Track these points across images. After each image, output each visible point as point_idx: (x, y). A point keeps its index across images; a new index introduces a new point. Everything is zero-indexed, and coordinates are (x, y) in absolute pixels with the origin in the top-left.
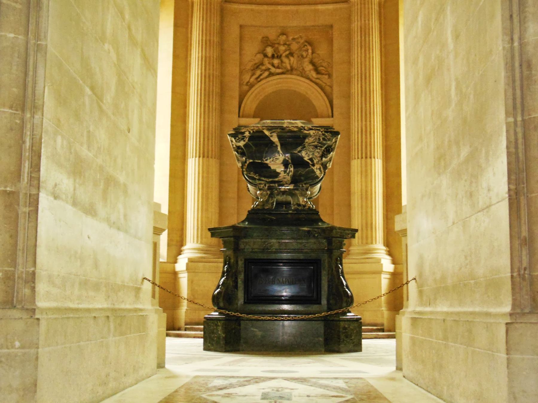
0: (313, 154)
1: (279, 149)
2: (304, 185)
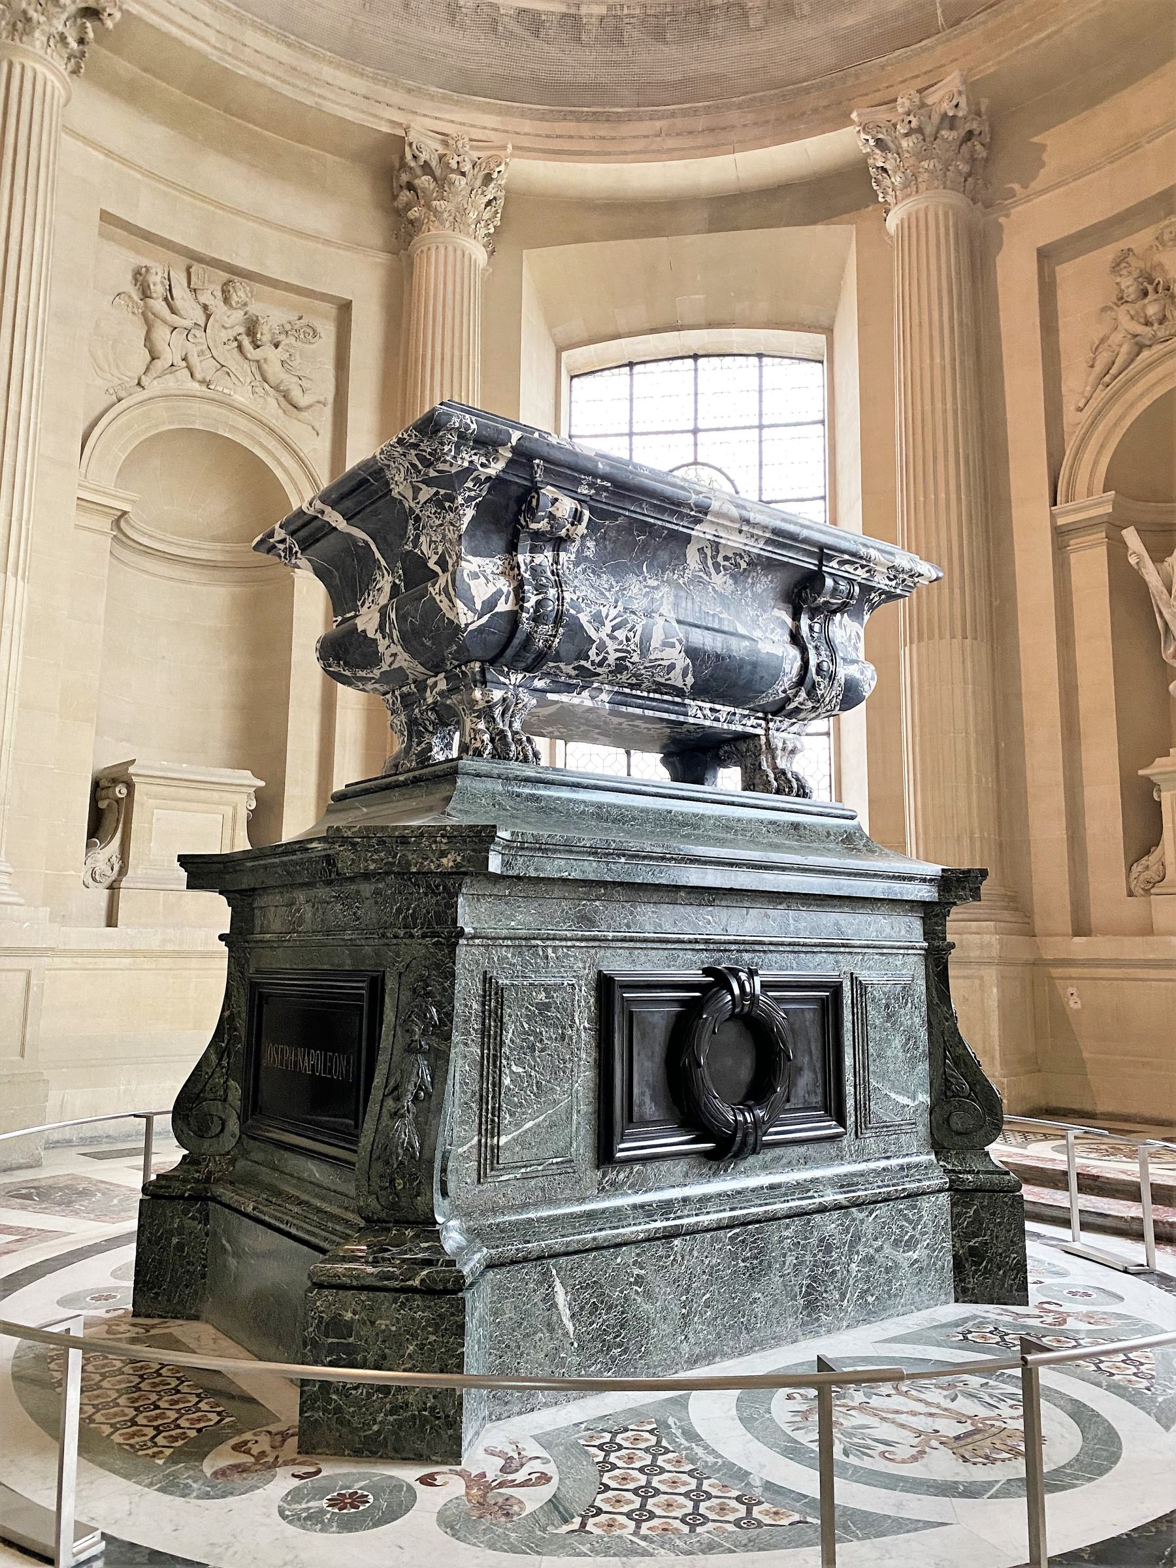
0: (444, 536)
1: (378, 555)
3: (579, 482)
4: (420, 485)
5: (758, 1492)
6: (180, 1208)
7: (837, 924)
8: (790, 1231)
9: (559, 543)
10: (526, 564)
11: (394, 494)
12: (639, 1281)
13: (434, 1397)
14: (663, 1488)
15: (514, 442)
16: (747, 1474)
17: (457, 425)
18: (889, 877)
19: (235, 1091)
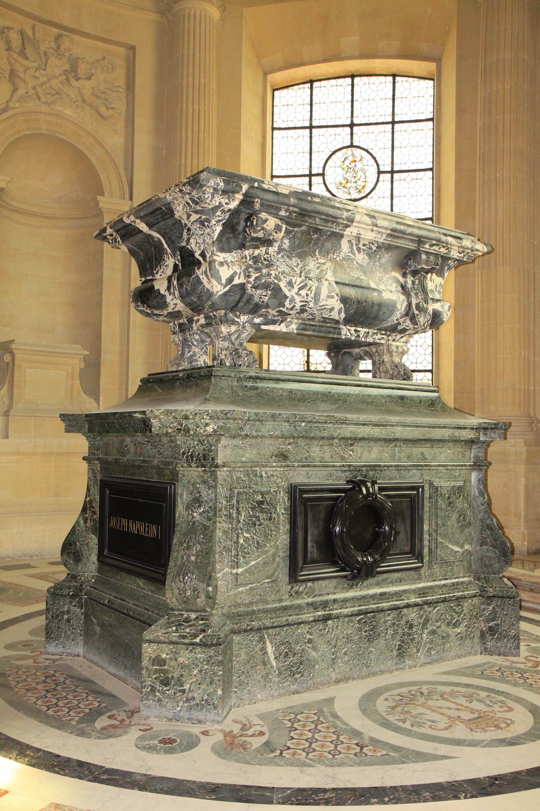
0: (204, 241)
1: (166, 246)
2: (215, 313)
3: (280, 209)
4: (192, 213)
5: (366, 741)
6: (68, 600)
7: (422, 454)
8: (390, 618)
9: (267, 242)
10: (250, 256)
11: (177, 216)
12: (310, 641)
13: (207, 695)
14: (319, 739)
15: (244, 191)
16: (362, 733)
17: (213, 184)
18: (452, 428)
19: (94, 540)
